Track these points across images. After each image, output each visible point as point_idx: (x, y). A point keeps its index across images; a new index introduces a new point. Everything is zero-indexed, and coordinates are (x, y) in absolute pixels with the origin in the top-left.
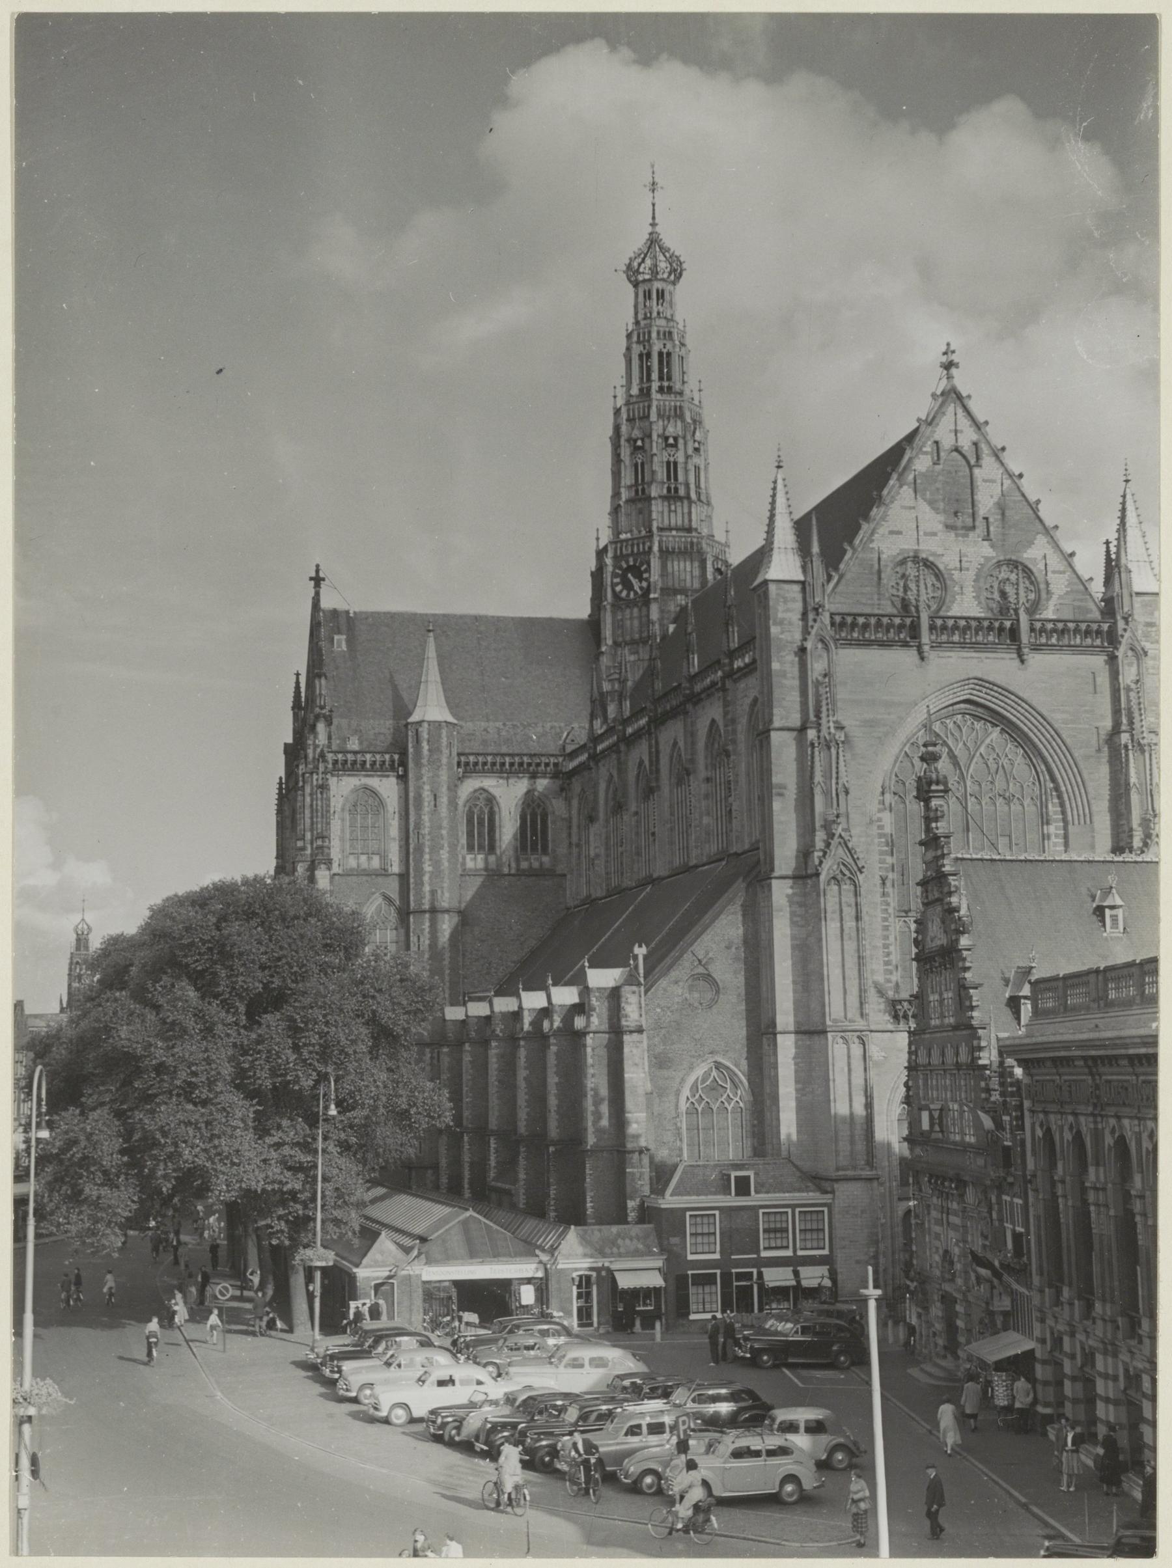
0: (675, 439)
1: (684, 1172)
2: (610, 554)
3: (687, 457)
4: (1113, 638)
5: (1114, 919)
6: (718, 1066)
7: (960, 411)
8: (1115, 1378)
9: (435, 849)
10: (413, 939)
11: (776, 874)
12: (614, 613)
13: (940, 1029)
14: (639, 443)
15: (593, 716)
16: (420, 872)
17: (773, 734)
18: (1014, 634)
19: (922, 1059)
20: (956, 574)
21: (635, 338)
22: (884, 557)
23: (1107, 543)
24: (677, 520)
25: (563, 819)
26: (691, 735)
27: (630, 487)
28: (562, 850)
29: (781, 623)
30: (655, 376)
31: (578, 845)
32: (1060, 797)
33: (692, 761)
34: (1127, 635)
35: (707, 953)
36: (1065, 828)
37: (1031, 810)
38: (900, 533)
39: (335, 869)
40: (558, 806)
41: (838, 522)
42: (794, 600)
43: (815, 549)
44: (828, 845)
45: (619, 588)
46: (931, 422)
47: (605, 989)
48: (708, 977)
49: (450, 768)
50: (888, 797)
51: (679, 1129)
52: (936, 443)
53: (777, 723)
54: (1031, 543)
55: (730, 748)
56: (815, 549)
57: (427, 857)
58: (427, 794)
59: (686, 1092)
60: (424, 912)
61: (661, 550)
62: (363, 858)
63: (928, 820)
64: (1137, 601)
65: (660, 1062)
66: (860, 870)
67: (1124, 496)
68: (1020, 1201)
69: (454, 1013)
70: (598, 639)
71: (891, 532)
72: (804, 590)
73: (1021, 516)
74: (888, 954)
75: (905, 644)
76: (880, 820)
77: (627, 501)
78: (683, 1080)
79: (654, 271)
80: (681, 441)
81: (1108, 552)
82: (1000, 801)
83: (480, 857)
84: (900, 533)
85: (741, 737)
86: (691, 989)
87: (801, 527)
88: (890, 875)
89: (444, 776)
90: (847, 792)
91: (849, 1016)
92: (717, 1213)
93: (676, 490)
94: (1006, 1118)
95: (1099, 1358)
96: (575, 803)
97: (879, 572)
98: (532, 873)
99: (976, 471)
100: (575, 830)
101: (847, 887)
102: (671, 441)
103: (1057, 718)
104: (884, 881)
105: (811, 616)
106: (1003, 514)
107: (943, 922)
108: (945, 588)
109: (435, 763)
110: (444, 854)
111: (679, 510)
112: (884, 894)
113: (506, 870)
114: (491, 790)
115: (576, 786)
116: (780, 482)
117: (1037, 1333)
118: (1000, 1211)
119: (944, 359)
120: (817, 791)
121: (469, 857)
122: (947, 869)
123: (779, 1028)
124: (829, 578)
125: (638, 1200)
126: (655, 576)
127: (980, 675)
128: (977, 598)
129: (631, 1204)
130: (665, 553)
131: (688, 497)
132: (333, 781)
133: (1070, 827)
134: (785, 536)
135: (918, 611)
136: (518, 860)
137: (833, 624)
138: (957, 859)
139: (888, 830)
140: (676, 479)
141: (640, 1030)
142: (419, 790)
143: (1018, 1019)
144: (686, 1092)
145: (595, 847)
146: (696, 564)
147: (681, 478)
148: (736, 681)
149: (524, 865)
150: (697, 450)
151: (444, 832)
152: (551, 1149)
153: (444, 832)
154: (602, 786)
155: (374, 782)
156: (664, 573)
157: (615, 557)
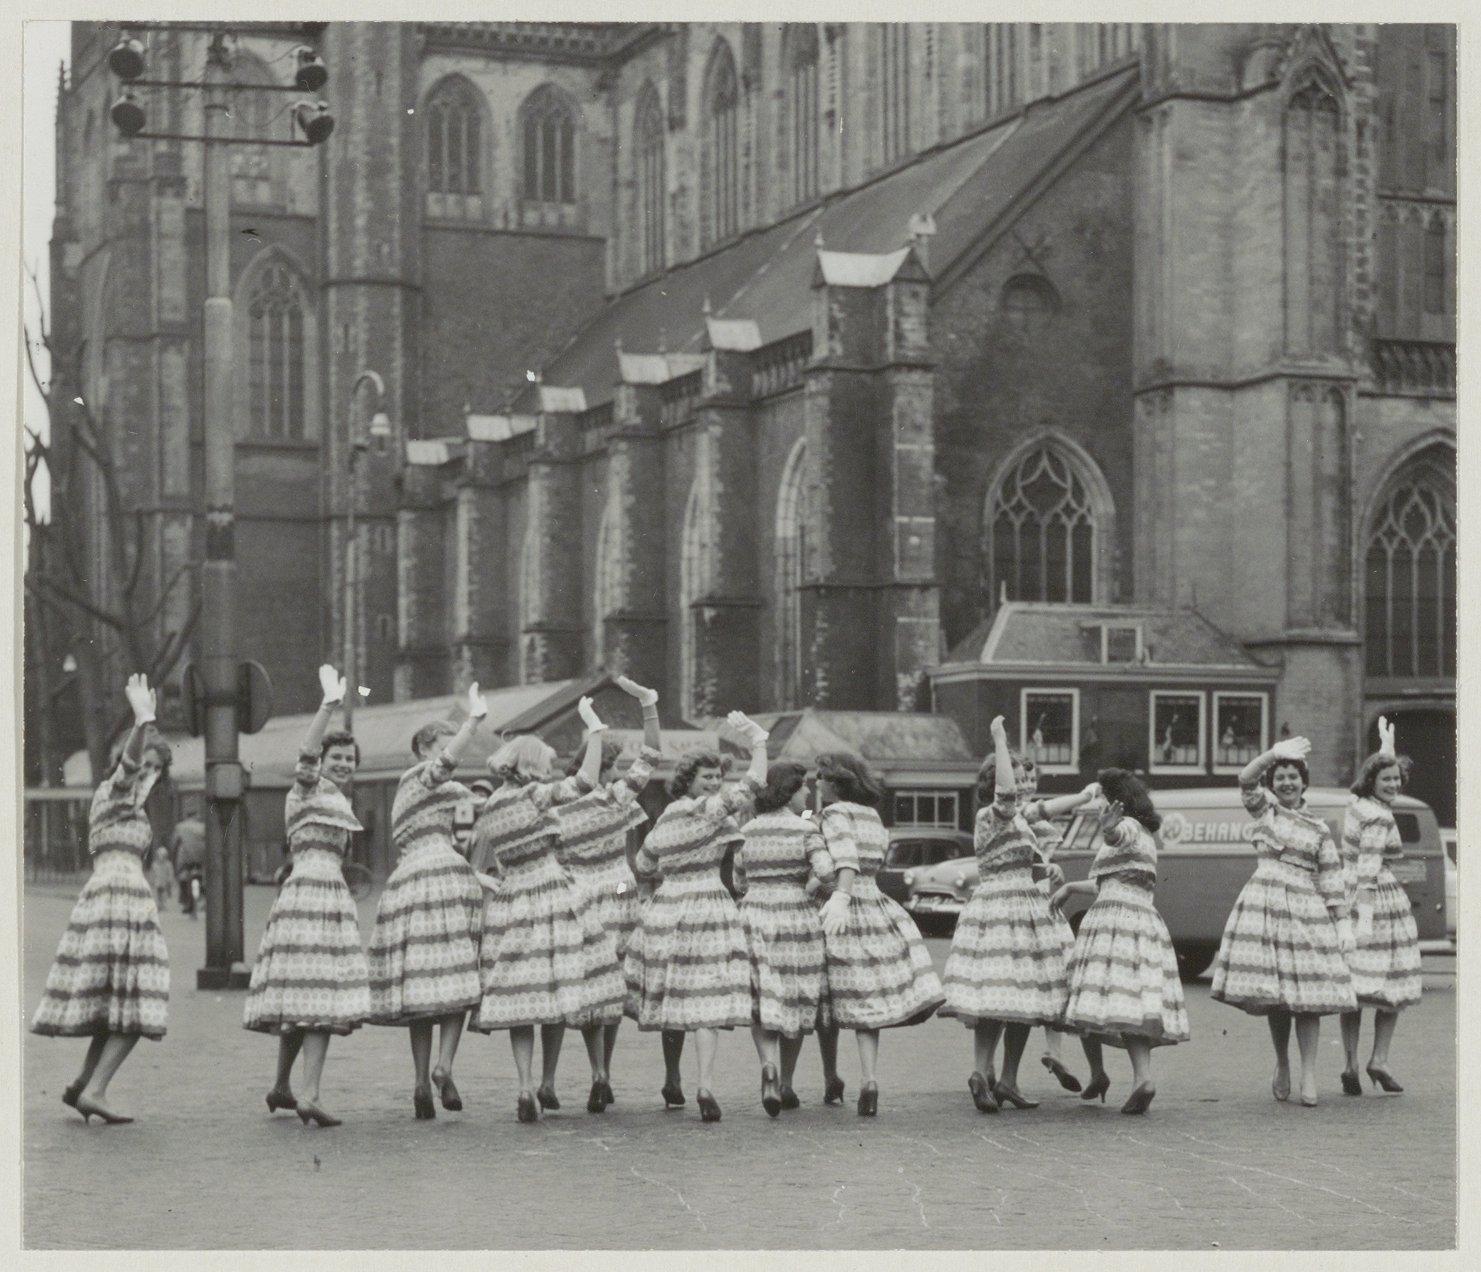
10: (336, 331)
25: (603, 141)
28: (598, 195)
31: (632, 184)
40: (593, 115)
51: (983, 556)
59: (995, 491)
65: (956, 435)
78: (993, 468)
83: (451, 199)
86: (1004, 305)
92: (1075, 692)
98: (542, 234)
113: (499, 224)
115: (632, 75)
121: (432, 197)
125: (917, 674)
129: (905, 681)
136: (521, 209)
149: (531, 218)
153: (394, 141)
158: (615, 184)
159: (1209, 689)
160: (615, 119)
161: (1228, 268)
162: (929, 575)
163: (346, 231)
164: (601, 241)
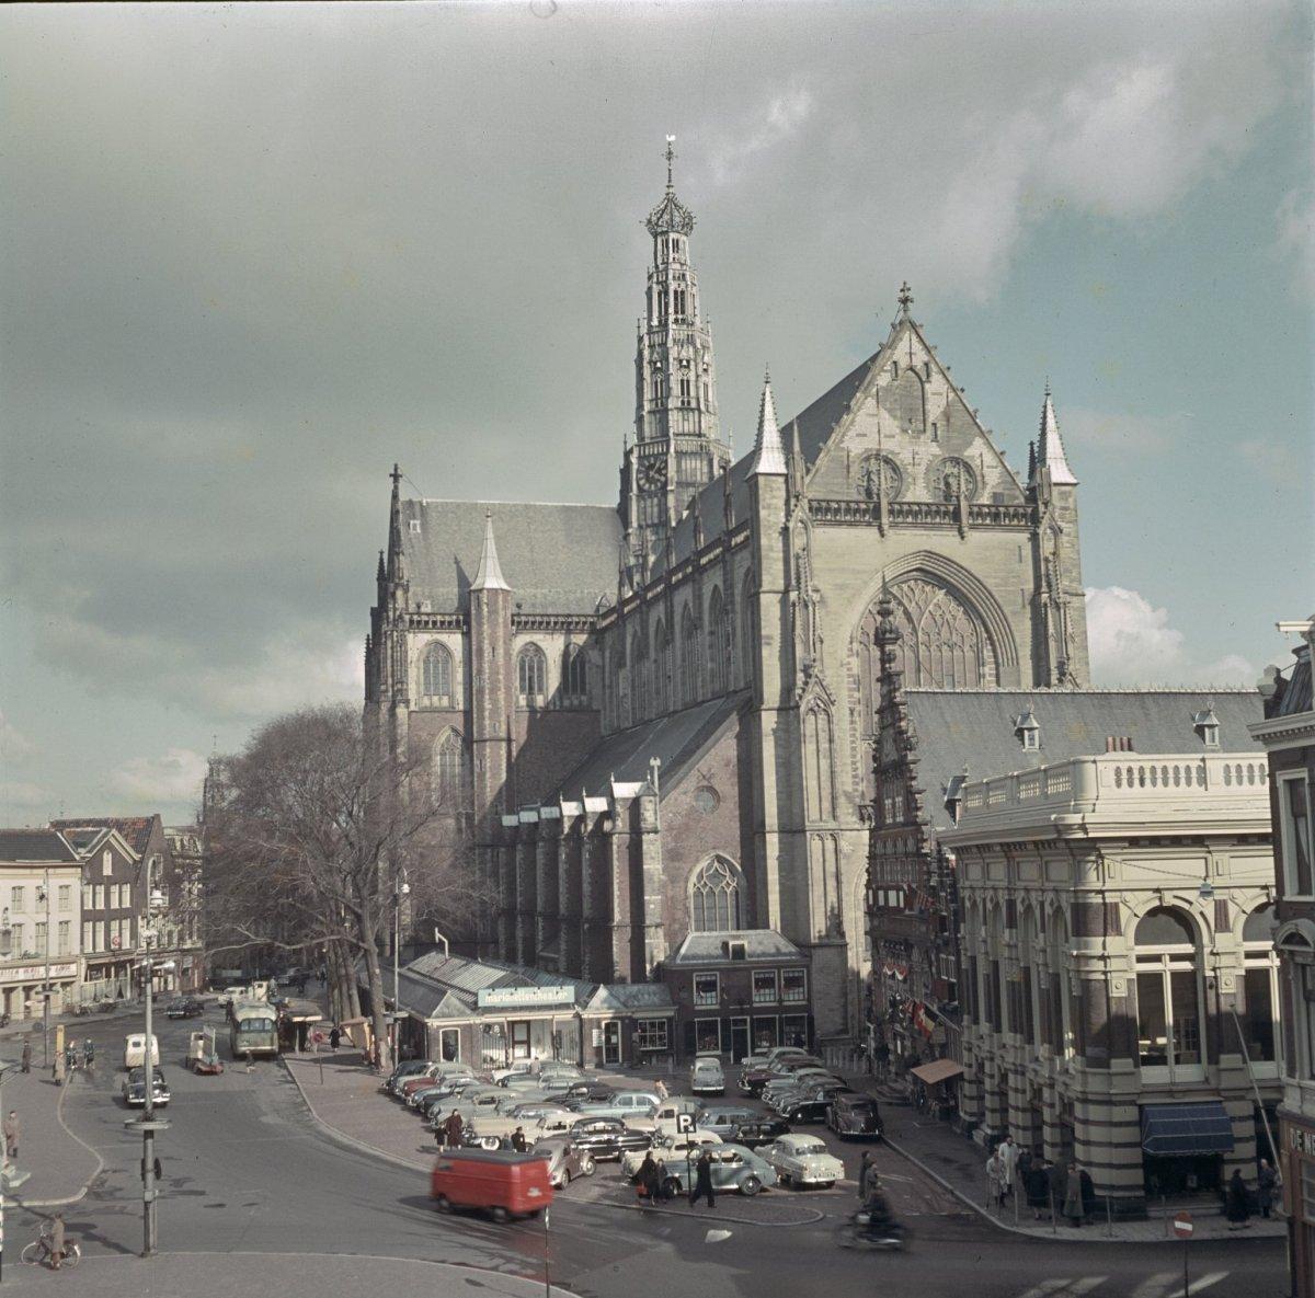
0: (688, 362)
1: (692, 942)
2: (635, 454)
3: (697, 376)
4: (1035, 519)
5: (1032, 739)
6: (720, 859)
7: (914, 337)
8: (1024, 1092)
9: (494, 690)
10: (476, 762)
11: (764, 707)
12: (638, 501)
13: (895, 825)
14: (659, 365)
15: (621, 585)
16: (481, 709)
17: (762, 596)
18: (956, 516)
19: (878, 852)
20: (910, 468)
21: (655, 280)
22: (852, 454)
23: (1032, 444)
24: (689, 427)
26: (698, 597)
27: (651, 401)
29: (769, 507)
30: (671, 310)
32: (992, 644)
33: (701, 619)
34: (1047, 516)
35: (710, 770)
36: (997, 669)
37: (970, 655)
38: (865, 435)
39: (413, 707)
40: (594, 655)
41: (815, 426)
42: (779, 489)
43: (797, 447)
44: (806, 683)
45: (642, 482)
46: (891, 345)
47: (628, 799)
48: (711, 789)
49: (506, 626)
50: (856, 646)
52: (895, 363)
53: (765, 587)
54: (969, 444)
55: (729, 607)
56: (797, 447)
57: (487, 697)
58: (486, 646)
59: (693, 879)
60: (491, 740)
61: (676, 452)
62: (435, 698)
63: (883, 662)
64: (1055, 490)
65: (673, 856)
66: (833, 703)
67: (1045, 407)
68: (953, 958)
69: (509, 821)
70: (626, 523)
71: (858, 435)
72: (786, 482)
73: (963, 420)
74: (856, 770)
75: (869, 524)
76: (849, 663)
77: (649, 412)
78: (691, 870)
79: (671, 224)
80: (692, 363)
81: (1032, 451)
82: (945, 648)
84: (865, 435)
85: (738, 599)
86: (697, 798)
87: (786, 433)
88: (858, 708)
89: (501, 632)
90: (822, 642)
91: (824, 818)
93: (689, 403)
94: (943, 894)
95: (1011, 1077)
96: (607, 654)
97: (848, 466)
98: (571, 710)
99: (927, 386)
100: (607, 675)
101: (822, 717)
102: (685, 363)
103: (990, 583)
104: (852, 712)
105: (793, 501)
106: (948, 421)
107: (895, 741)
108: (901, 479)
109: (494, 625)
110: (501, 695)
111: (691, 419)
112: (852, 722)
114: (539, 643)
116: (768, 394)
117: (965, 1060)
118: (938, 968)
119: (901, 295)
120: (797, 641)
122: (898, 700)
123: (768, 829)
124: (808, 471)
126: (672, 472)
127: (928, 548)
128: (927, 487)
129: (648, 967)
130: (680, 454)
131: (699, 409)
132: (410, 637)
133: (1001, 668)
134: (771, 436)
135: (879, 498)
136: (561, 699)
137: (811, 509)
138: (906, 693)
139: (855, 671)
140: (688, 394)
141: (656, 832)
142: (480, 643)
143: (954, 817)
144: (693, 879)
145: (624, 688)
146: (705, 463)
147: (692, 393)
148: (733, 554)
149: (566, 703)
150: (705, 370)
151: (501, 677)
152: (586, 926)
153: (501, 677)
154: (629, 640)
155: (444, 637)
156: (679, 471)
157: (640, 458)
158: (604, 686)
159: (779, 968)
160: (603, 658)
161: (788, 781)
162: (659, 921)
163: (481, 718)
164: (599, 711)
